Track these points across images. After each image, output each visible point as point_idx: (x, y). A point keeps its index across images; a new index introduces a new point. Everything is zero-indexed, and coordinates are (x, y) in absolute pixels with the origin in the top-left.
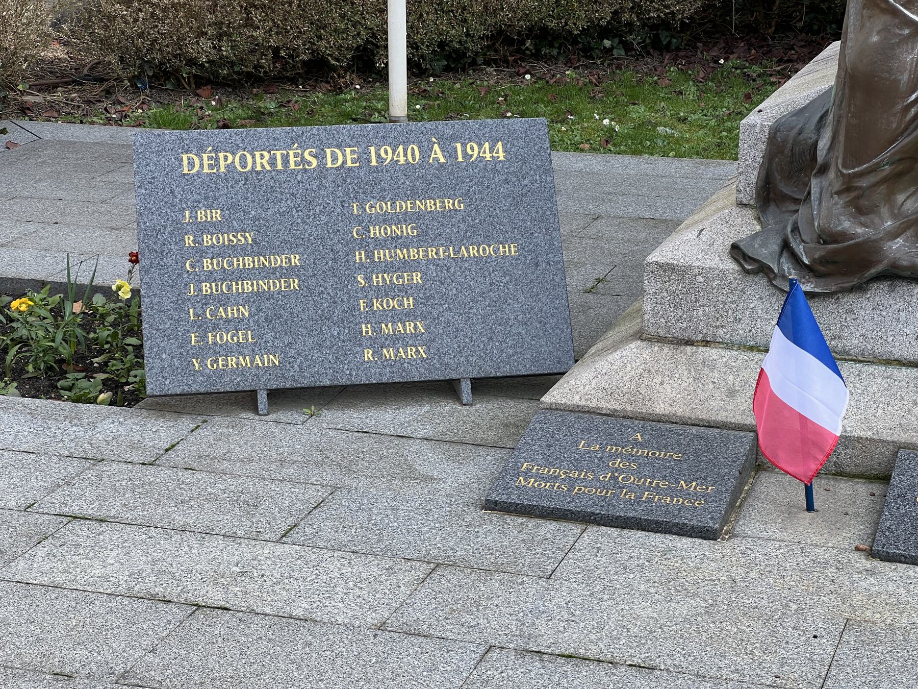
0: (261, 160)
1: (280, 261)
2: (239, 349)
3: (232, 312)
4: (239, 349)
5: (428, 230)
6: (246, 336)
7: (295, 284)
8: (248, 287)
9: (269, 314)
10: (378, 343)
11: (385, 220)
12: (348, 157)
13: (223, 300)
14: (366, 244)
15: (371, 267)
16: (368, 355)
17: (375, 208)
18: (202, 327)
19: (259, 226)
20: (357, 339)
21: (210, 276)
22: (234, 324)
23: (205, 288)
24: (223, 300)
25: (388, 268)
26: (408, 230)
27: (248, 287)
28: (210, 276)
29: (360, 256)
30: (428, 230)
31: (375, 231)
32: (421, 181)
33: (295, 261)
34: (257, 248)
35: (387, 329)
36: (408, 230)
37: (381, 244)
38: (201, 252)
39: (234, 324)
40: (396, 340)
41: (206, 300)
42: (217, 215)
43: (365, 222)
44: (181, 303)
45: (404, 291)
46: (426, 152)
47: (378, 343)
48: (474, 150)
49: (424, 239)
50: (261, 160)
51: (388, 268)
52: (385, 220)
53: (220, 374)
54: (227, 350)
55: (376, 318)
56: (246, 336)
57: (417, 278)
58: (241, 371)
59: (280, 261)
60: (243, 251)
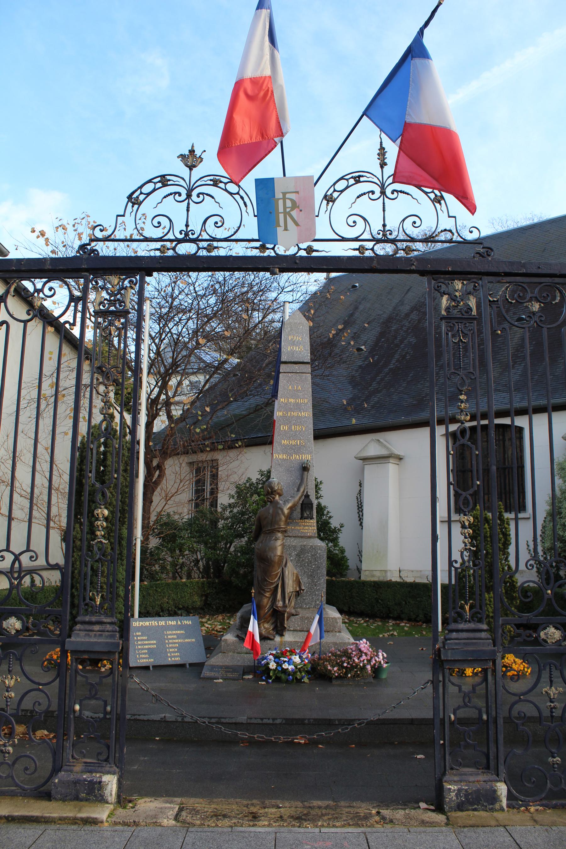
0: (147, 623)
1: (152, 642)
2: (146, 658)
3: (144, 651)
4: (146, 658)
5: (179, 636)
6: (147, 656)
7: (155, 646)
8: (147, 647)
9: (151, 652)
10: (171, 657)
11: (171, 635)
12: (163, 623)
13: (143, 649)
14: (168, 639)
15: (169, 643)
16: (170, 659)
17: (169, 632)
18: (139, 654)
19: (148, 636)
20: (168, 657)
21: (140, 645)
22: (145, 654)
23: (139, 647)
24: (143, 649)
25: (172, 643)
26: (175, 637)
27: (147, 647)
28: (140, 645)
29: (167, 641)
30: (179, 636)
31: (169, 637)
32: (178, 627)
33: (155, 642)
34: (147, 640)
35: (173, 654)
36: (175, 637)
37: (170, 639)
38: (138, 640)
39: (145, 654)
40: (174, 657)
41: (139, 649)
42: (140, 633)
43: (167, 635)
44: (135, 650)
45: (175, 647)
46: (177, 622)
47: (171, 657)
48: (185, 622)
49: (178, 638)
50: (147, 623)
51: (172, 643)
52: (171, 635)
53: (143, 663)
54: (144, 658)
55: (171, 653)
56: (147, 656)
57: (177, 645)
58: (147, 662)
59: (152, 642)
60: (145, 640)
